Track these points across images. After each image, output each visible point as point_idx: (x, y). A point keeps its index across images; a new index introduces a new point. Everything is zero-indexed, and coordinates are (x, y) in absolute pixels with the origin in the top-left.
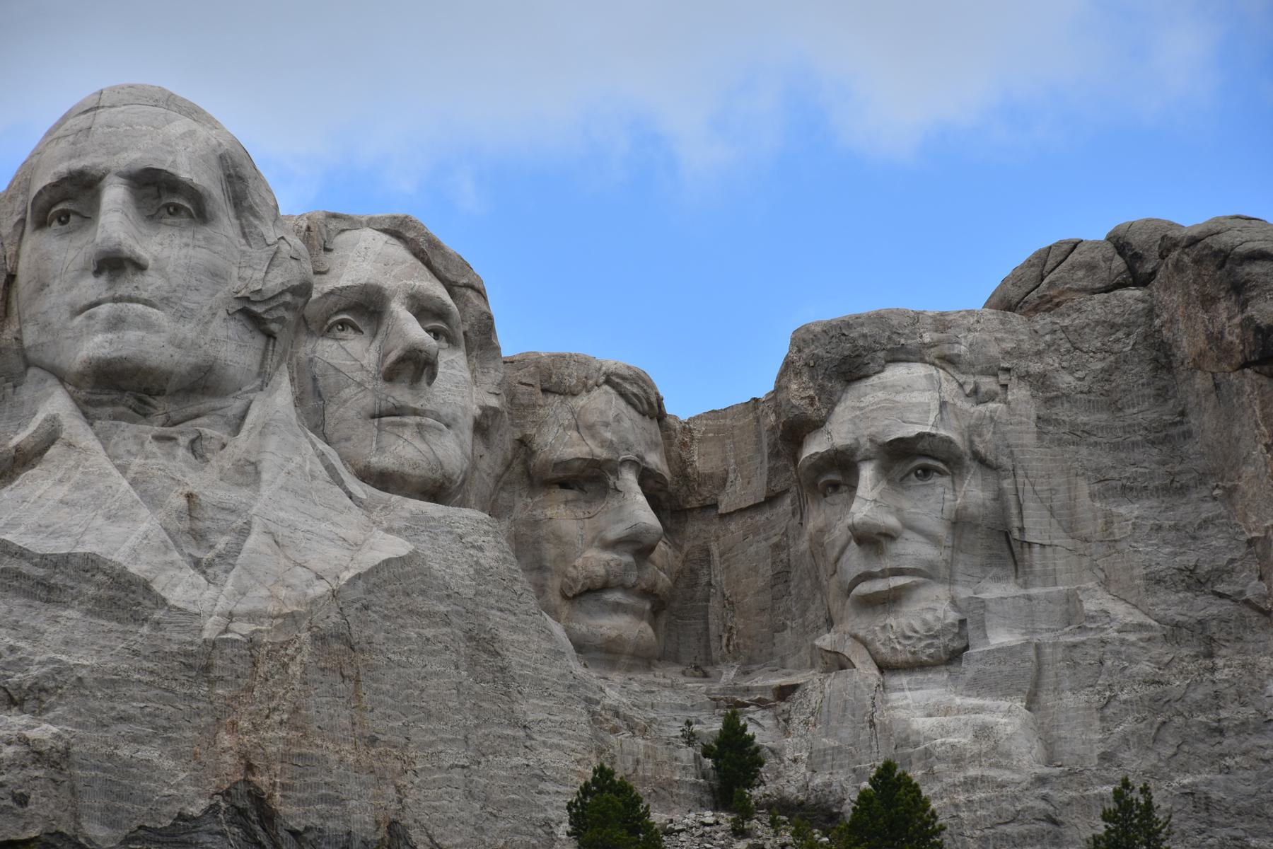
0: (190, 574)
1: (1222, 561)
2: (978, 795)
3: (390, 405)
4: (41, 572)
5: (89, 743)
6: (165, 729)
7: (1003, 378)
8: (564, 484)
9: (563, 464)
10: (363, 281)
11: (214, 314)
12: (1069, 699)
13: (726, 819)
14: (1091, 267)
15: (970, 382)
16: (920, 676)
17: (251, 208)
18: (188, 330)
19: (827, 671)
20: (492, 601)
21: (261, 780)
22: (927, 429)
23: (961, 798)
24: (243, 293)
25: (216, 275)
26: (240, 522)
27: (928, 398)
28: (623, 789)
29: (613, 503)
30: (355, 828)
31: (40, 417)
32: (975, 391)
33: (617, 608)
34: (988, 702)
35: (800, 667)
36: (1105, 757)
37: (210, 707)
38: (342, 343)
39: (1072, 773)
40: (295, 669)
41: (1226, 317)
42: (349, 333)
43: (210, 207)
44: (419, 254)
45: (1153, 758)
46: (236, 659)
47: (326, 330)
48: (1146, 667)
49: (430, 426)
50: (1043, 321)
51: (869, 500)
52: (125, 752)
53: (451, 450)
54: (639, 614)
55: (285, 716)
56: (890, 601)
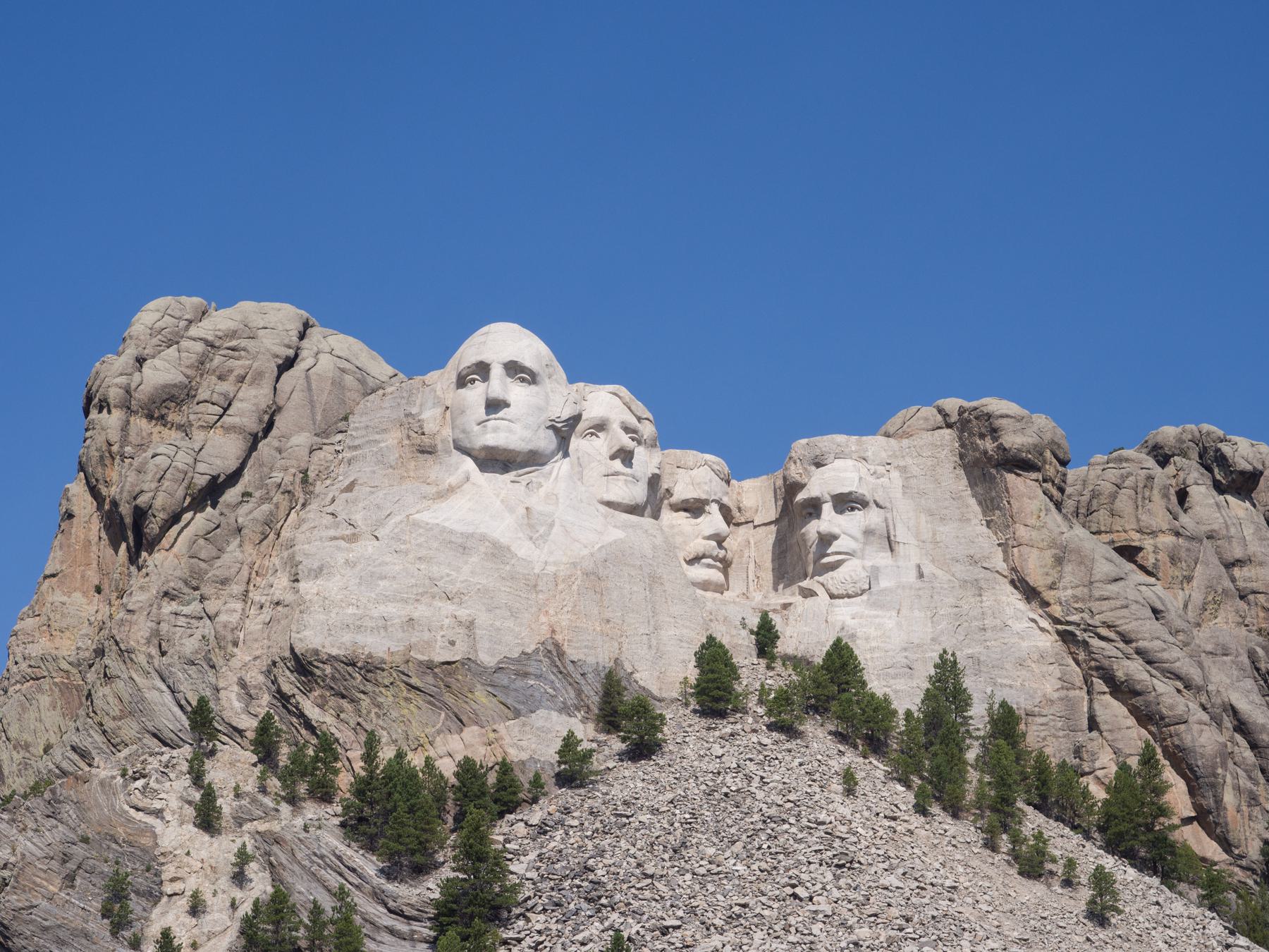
0: (528, 544)
1: (986, 554)
2: (876, 655)
4: (460, 541)
5: (483, 619)
7: (888, 467)
8: (685, 510)
9: (686, 501)
12: (917, 613)
13: (763, 662)
14: (926, 419)
15: (872, 468)
16: (846, 600)
18: (527, 434)
19: (805, 597)
21: (559, 637)
22: (854, 489)
23: (868, 656)
27: (855, 476)
28: (721, 646)
30: (600, 660)
31: (460, 471)
33: (709, 566)
34: (880, 613)
35: (793, 594)
36: (933, 640)
39: (918, 646)
40: (575, 587)
41: (988, 445)
43: (538, 379)
45: (954, 641)
48: (952, 601)
50: (905, 442)
51: (829, 520)
52: (498, 624)
53: (638, 493)
54: (718, 568)
56: (834, 566)
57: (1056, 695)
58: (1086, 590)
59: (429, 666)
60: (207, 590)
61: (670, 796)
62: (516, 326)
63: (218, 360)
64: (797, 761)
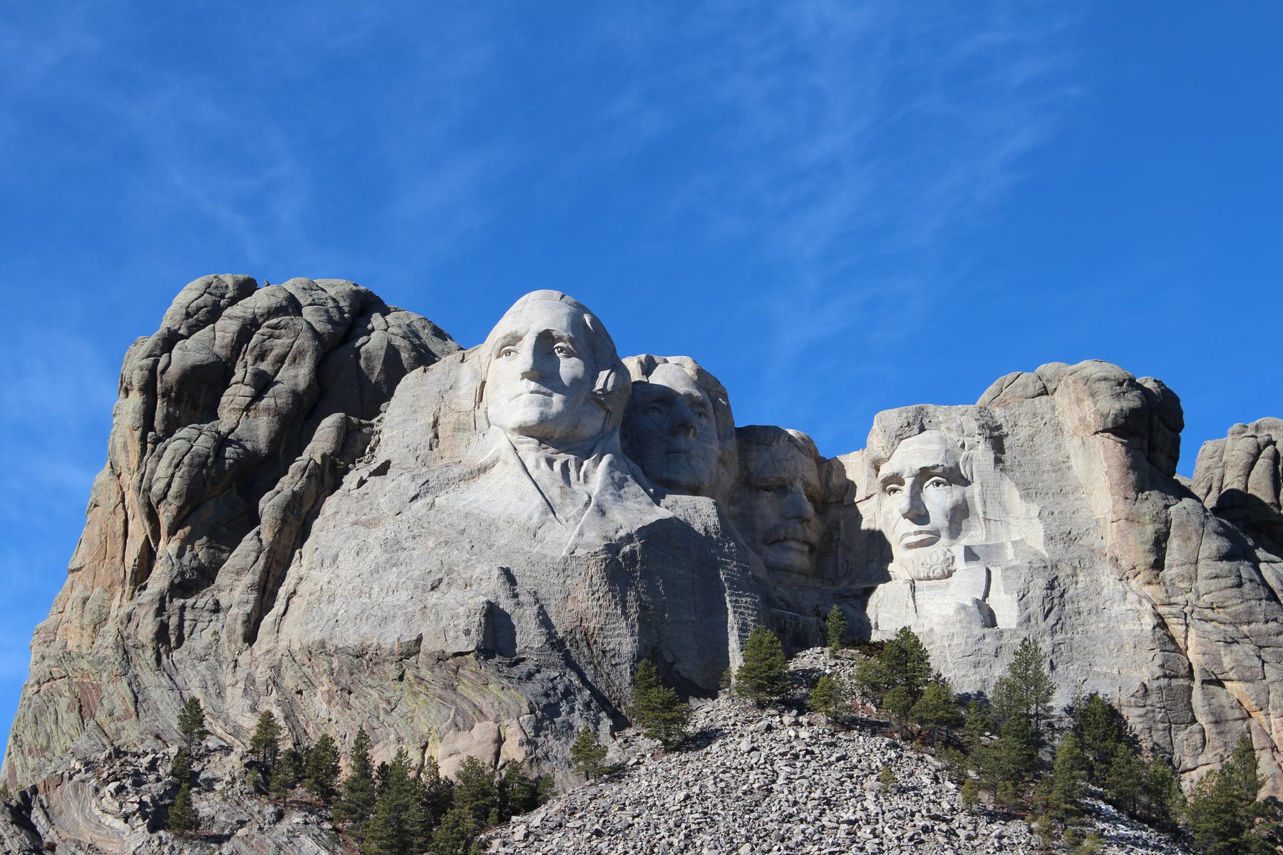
2: (955, 642)
7: (977, 438)
8: (767, 490)
12: (1003, 596)
14: (1026, 386)
26: (586, 498)
29: (789, 498)
32: (963, 446)
33: (790, 549)
36: (1020, 624)
48: (1041, 582)
54: (802, 552)
57: (1156, 684)
58: (1192, 568)
59: (441, 658)
60: (222, 578)
61: (681, 795)
62: (557, 294)
63: (256, 338)
64: (833, 759)
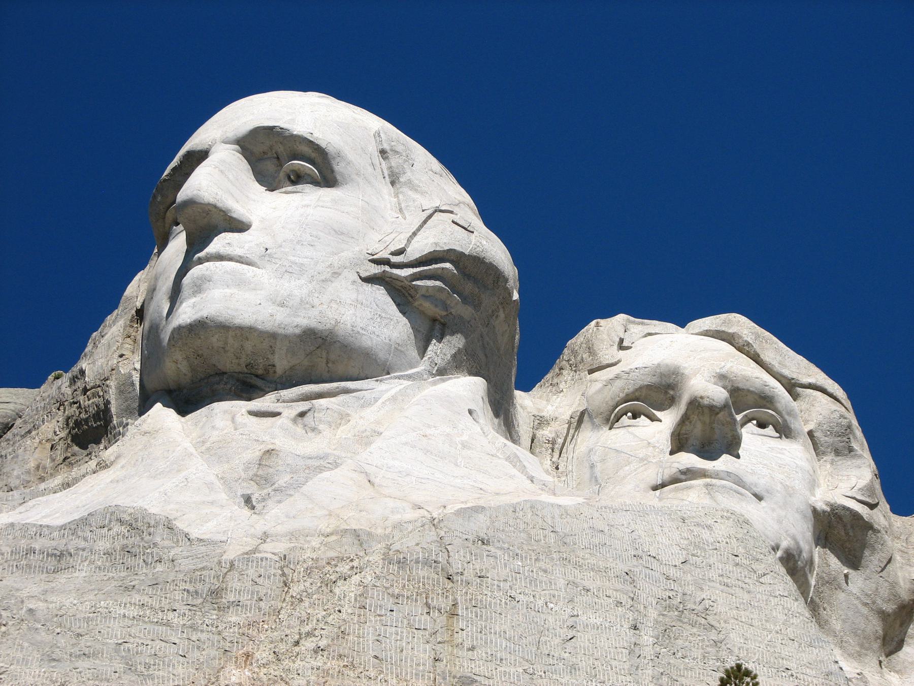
3: (674, 470)
6: (147, 666)
10: (656, 362)
11: (336, 274)
17: (410, 182)
18: (296, 288)
20: (713, 574)
24: (385, 255)
25: (340, 233)
37: (216, 637)
38: (631, 429)
42: (643, 420)
44: (740, 350)
46: (260, 581)
47: (612, 419)
49: (724, 487)
55: (323, 643)
